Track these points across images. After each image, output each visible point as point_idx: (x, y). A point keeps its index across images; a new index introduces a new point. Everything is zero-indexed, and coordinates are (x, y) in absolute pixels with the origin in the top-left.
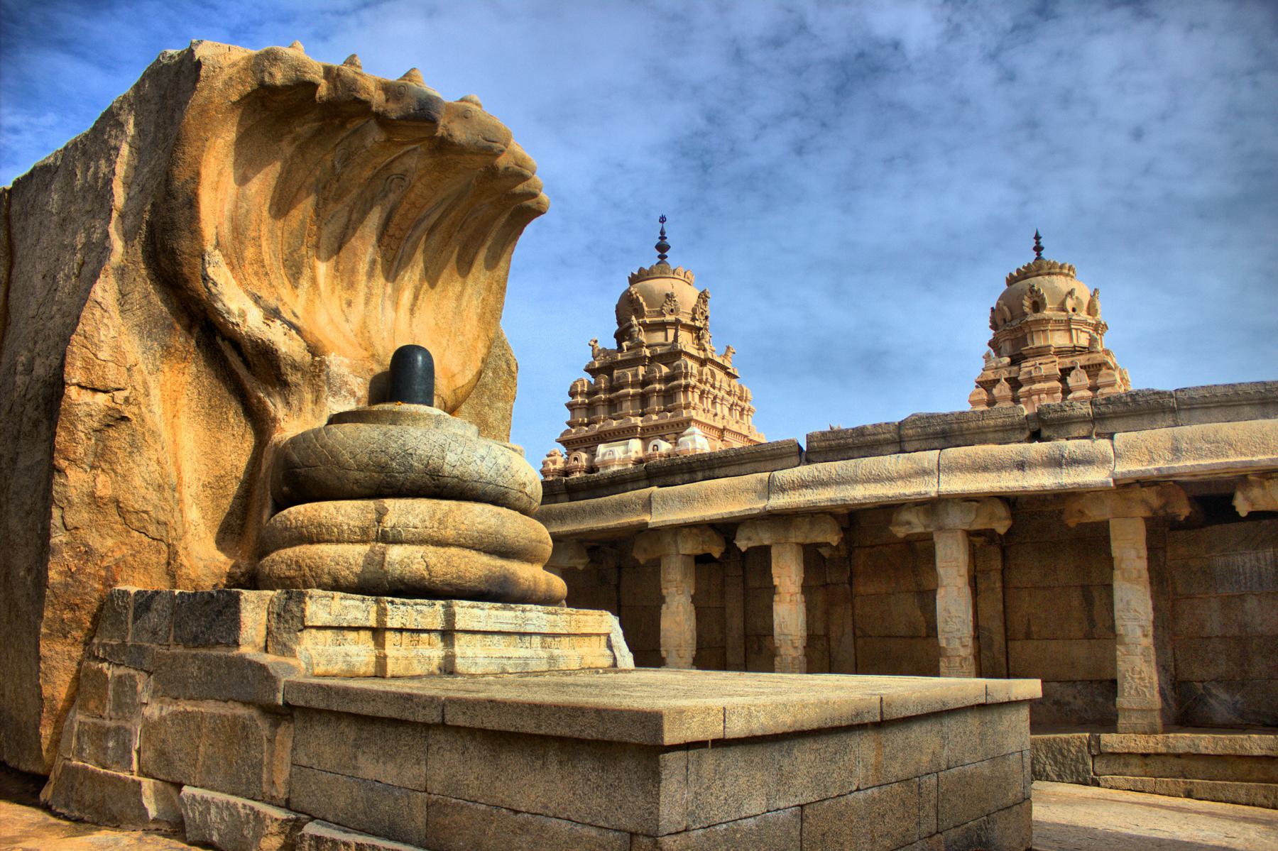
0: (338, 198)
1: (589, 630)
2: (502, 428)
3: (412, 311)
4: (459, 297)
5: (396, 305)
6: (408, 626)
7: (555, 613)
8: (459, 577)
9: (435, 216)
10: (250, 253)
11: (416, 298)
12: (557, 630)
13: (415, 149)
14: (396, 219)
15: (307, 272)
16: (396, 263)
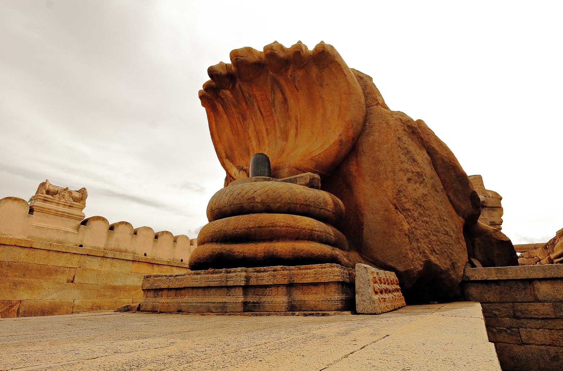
0: (244, 119)
1: (310, 280)
2: (388, 158)
3: (296, 135)
4: (324, 115)
5: (286, 139)
6: (171, 287)
7: (265, 271)
8: (198, 259)
9: (279, 96)
10: (236, 154)
11: (297, 129)
12: (264, 283)
13: (239, 84)
14: (262, 110)
15: (250, 148)
16: (277, 124)
